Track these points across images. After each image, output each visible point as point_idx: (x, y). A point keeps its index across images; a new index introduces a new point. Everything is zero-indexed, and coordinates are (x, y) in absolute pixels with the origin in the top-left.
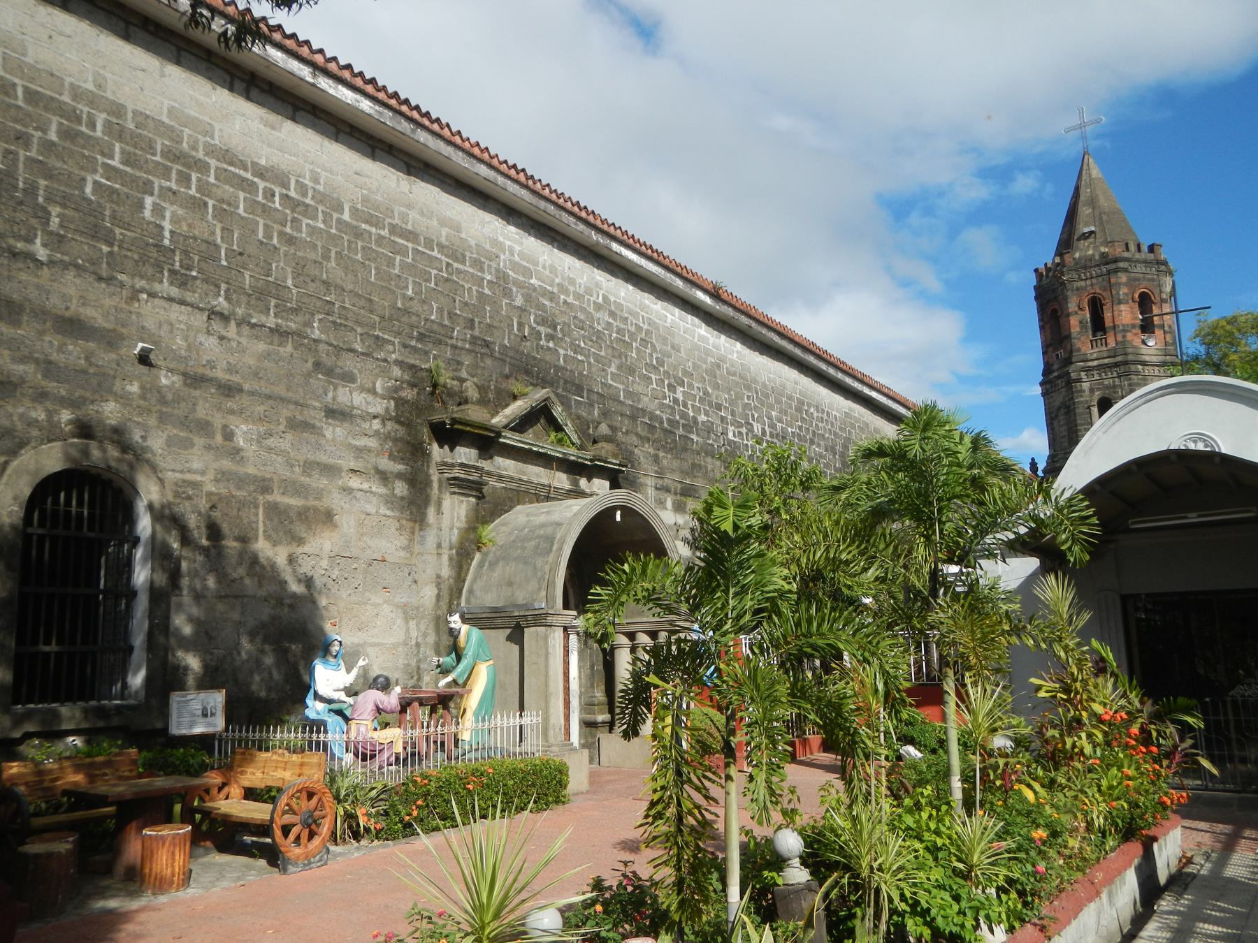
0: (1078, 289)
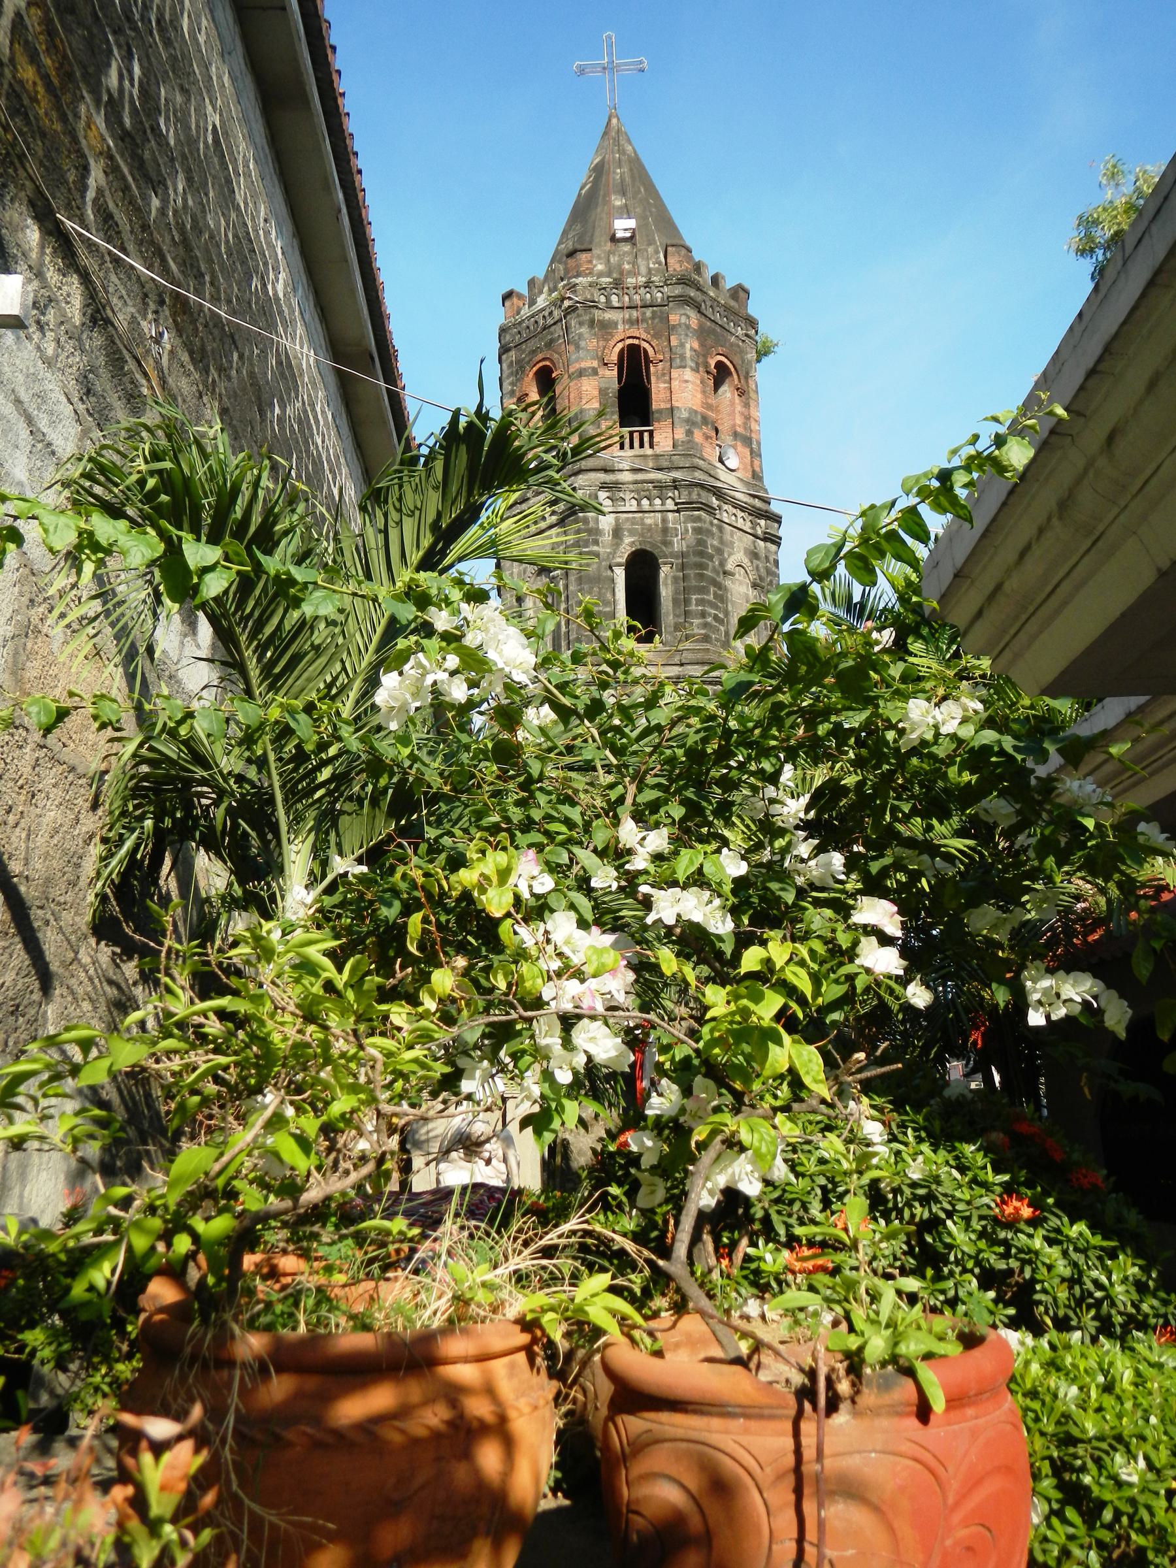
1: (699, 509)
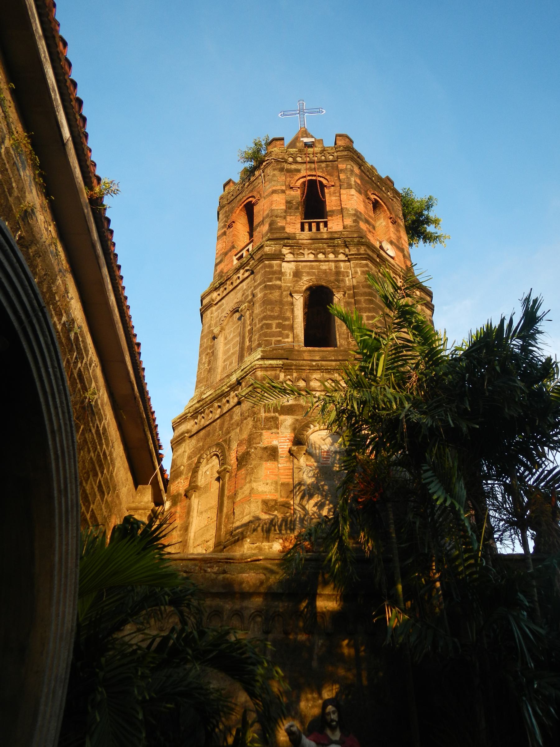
0: (289, 171)
1: (365, 259)
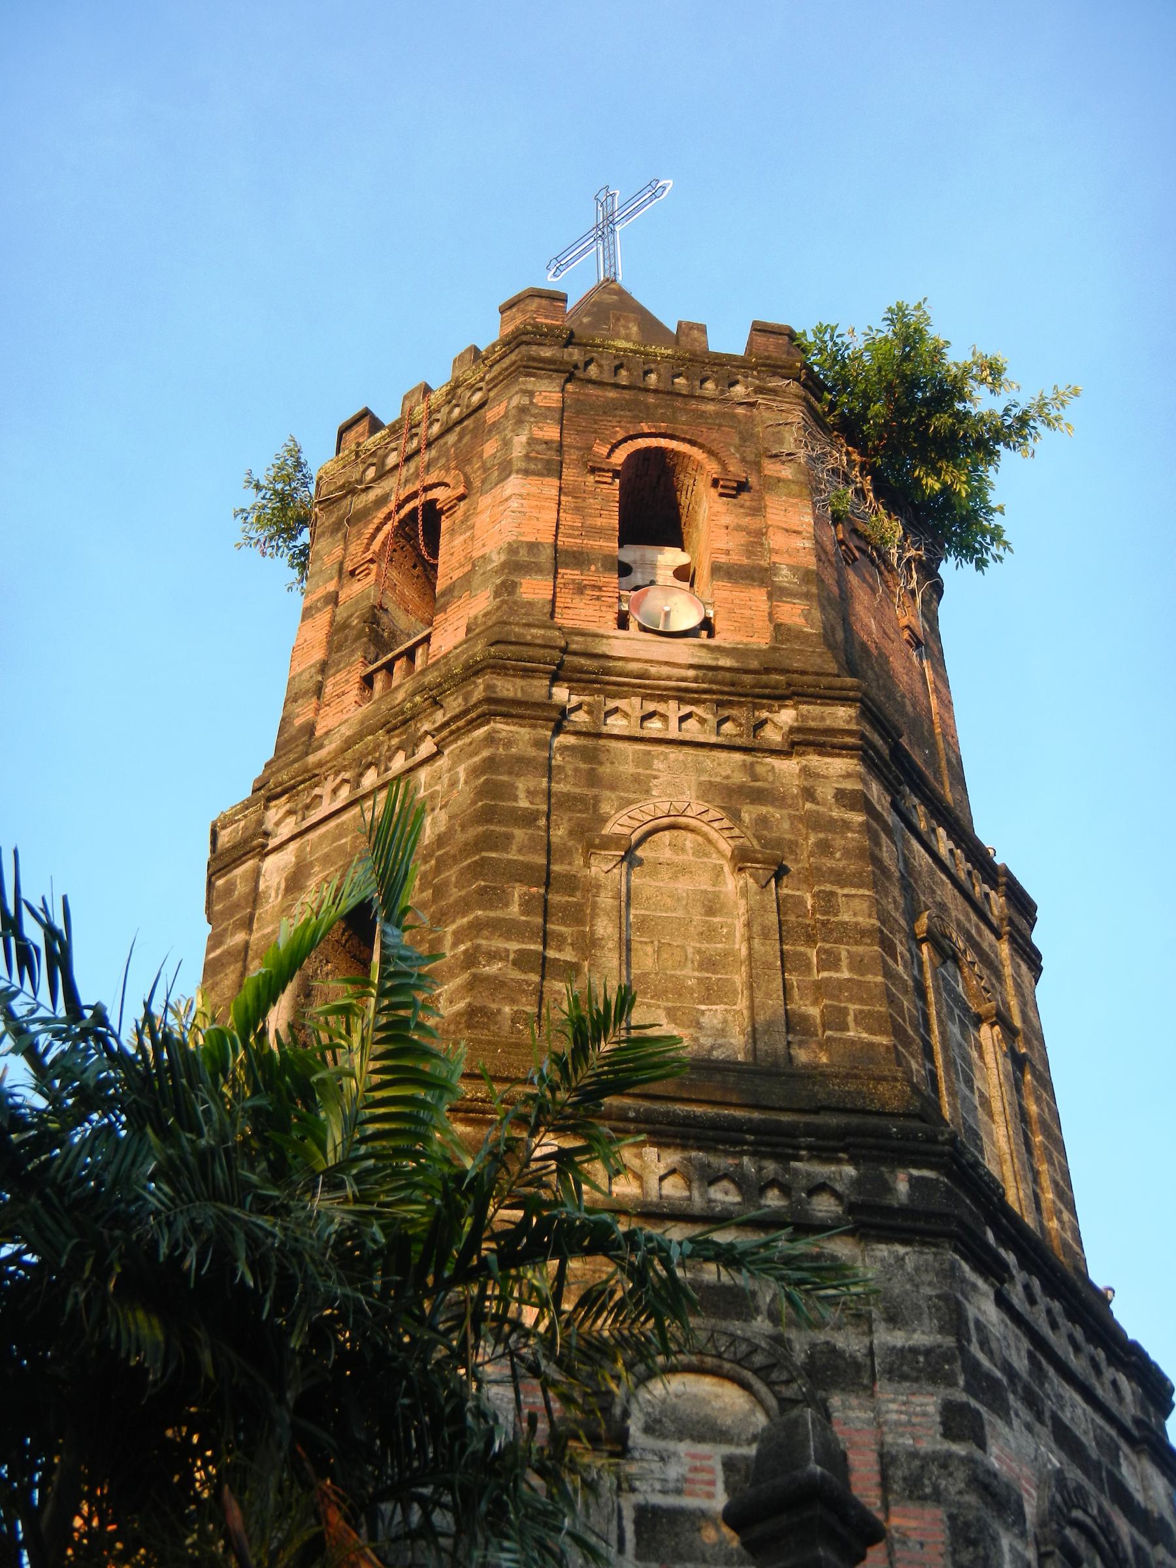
1: (484, 718)
